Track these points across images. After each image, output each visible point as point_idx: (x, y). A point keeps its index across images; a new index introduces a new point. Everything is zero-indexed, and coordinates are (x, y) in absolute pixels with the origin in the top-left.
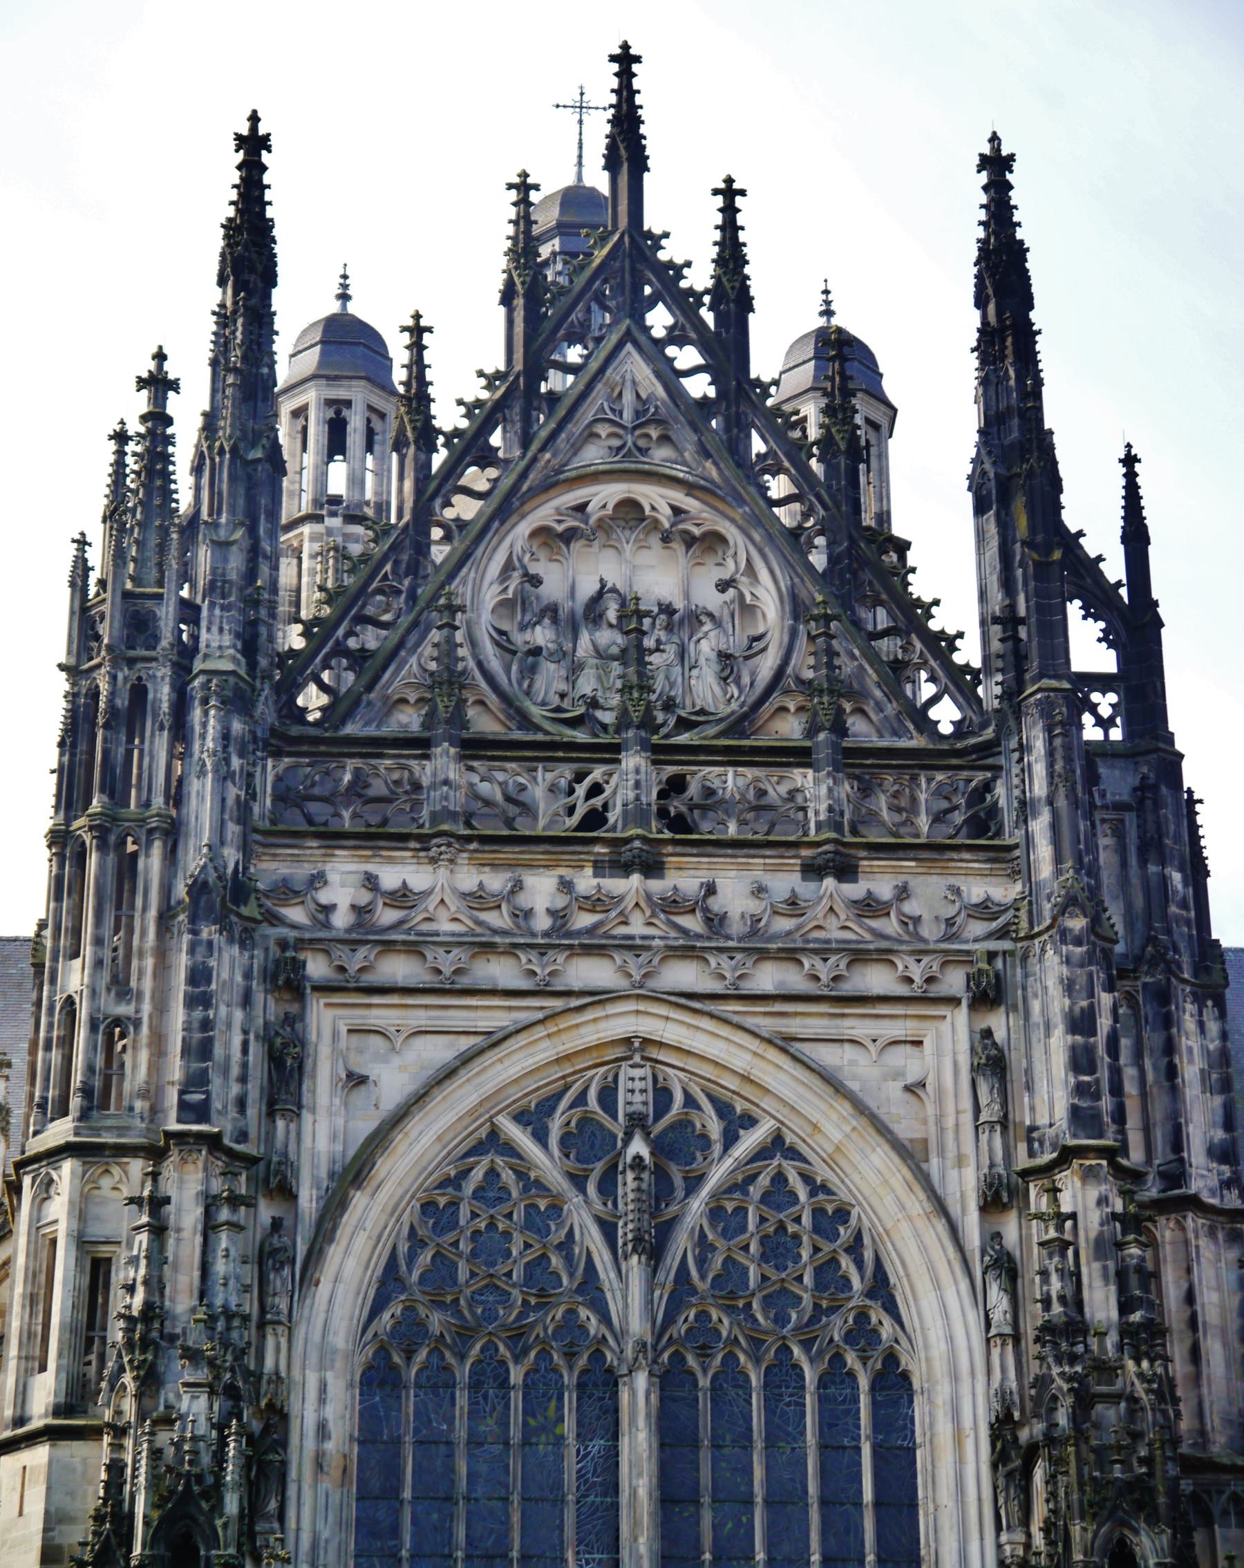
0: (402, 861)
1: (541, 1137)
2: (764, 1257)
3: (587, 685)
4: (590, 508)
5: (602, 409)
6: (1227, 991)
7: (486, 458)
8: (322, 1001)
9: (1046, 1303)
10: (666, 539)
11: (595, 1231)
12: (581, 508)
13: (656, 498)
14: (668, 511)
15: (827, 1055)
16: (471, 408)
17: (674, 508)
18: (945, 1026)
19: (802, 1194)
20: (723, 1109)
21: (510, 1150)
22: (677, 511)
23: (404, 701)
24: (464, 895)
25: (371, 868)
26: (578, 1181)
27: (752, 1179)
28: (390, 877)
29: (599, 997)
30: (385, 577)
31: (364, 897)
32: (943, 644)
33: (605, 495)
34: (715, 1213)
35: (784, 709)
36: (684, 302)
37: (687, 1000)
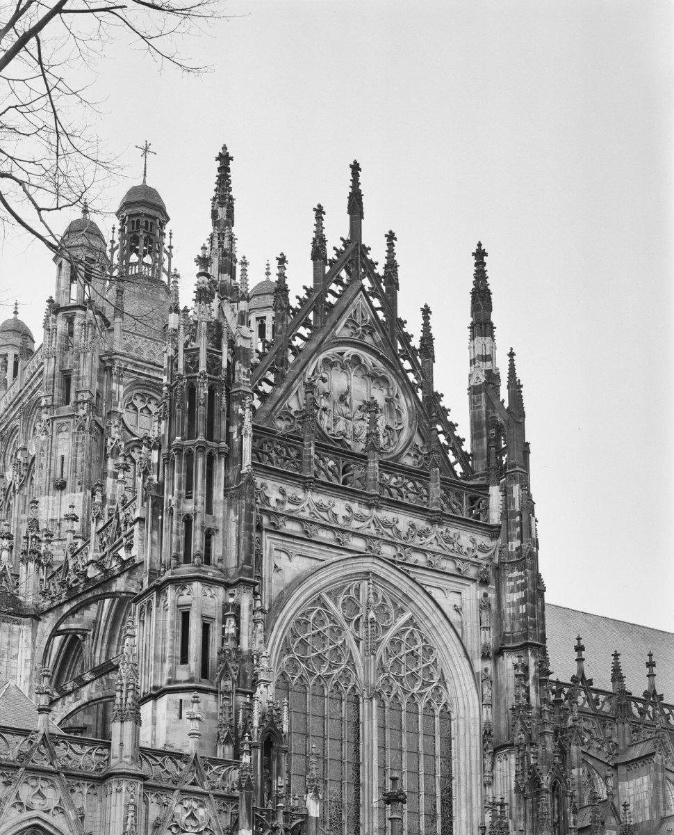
0: (295, 486)
1: (336, 602)
2: (408, 661)
3: (341, 426)
4: (345, 355)
5: (351, 316)
6: (545, 593)
7: (307, 324)
8: (267, 535)
9: (517, 697)
10: (368, 376)
11: (354, 642)
12: (342, 354)
13: (368, 358)
14: (371, 364)
15: (436, 594)
16: (302, 302)
17: (373, 364)
18: (467, 588)
19: (419, 642)
20: (395, 604)
21: (324, 605)
22: (374, 365)
23: (280, 418)
24: (317, 504)
25: (284, 487)
26: (349, 621)
27: (405, 631)
28: (290, 491)
29: (359, 554)
30: (273, 364)
31: (280, 497)
32: (460, 441)
33: (350, 351)
34: (392, 642)
35: (409, 454)
36: (375, 279)
37: (392, 563)
